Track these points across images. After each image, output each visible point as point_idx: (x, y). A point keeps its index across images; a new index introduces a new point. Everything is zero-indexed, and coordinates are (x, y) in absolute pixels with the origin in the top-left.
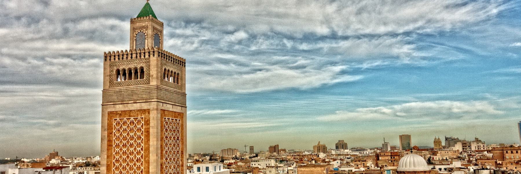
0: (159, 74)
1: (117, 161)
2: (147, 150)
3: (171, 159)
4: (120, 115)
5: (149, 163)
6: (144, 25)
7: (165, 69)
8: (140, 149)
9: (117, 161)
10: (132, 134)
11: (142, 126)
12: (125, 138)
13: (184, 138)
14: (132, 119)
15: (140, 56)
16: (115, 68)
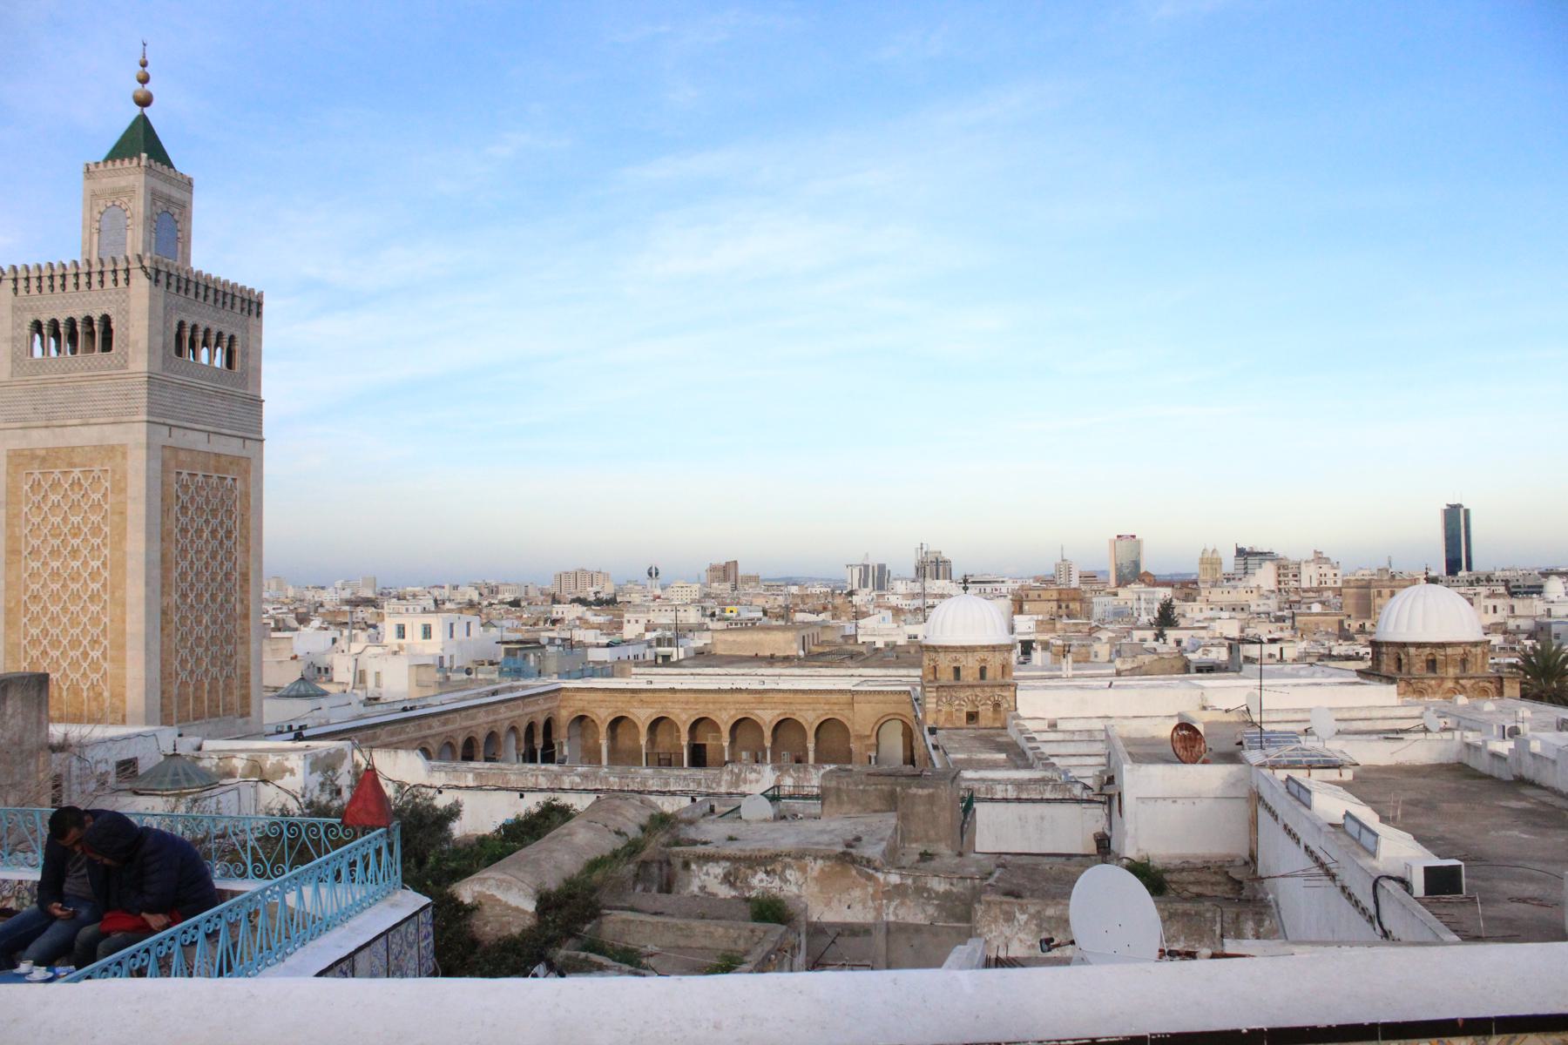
0: (160, 339)
1: (35, 598)
2: (119, 566)
3: (199, 596)
4: (44, 460)
5: (124, 605)
6: (123, 184)
7: (181, 325)
8: (99, 563)
9: (35, 598)
10: (76, 519)
11: (105, 495)
12: (55, 532)
13: (253, 534)
14: (76, 472)
15: (102, 282)
16: (29, 318)
